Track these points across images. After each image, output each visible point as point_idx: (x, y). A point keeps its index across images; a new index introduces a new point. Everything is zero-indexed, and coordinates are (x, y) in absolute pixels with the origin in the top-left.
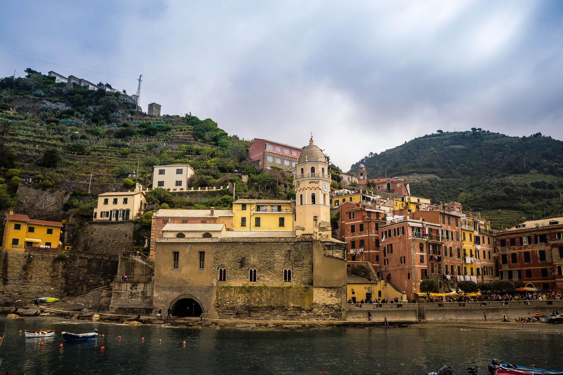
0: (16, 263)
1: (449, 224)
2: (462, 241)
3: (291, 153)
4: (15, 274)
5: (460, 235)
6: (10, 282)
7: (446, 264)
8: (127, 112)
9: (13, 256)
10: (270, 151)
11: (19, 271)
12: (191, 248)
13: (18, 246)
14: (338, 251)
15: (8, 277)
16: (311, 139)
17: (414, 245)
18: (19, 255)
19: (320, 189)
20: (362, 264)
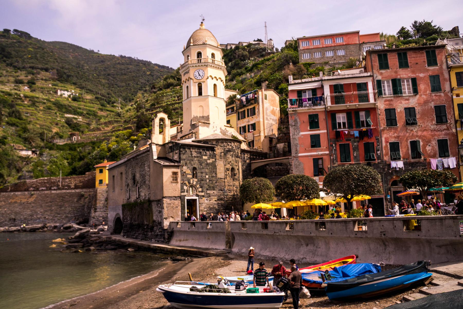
0: (102, 197)
1: (404, 64)
2: (452, 89)
3: (334, 42)
4: (101, 205)
5: (445, 80)
6: (98, 210)
7: (393, 140)
8: (258, 57)
9: (100, 192)
10: (306, 48)
11: (103, 202)
12: (118, 171)
13: (102, 185)
14: (176, 152)
15: (97, 207)
16: (202, 23)
17: (296, 121)
18: (103, 191)
19: (191, 79)
20: (282, 160)
